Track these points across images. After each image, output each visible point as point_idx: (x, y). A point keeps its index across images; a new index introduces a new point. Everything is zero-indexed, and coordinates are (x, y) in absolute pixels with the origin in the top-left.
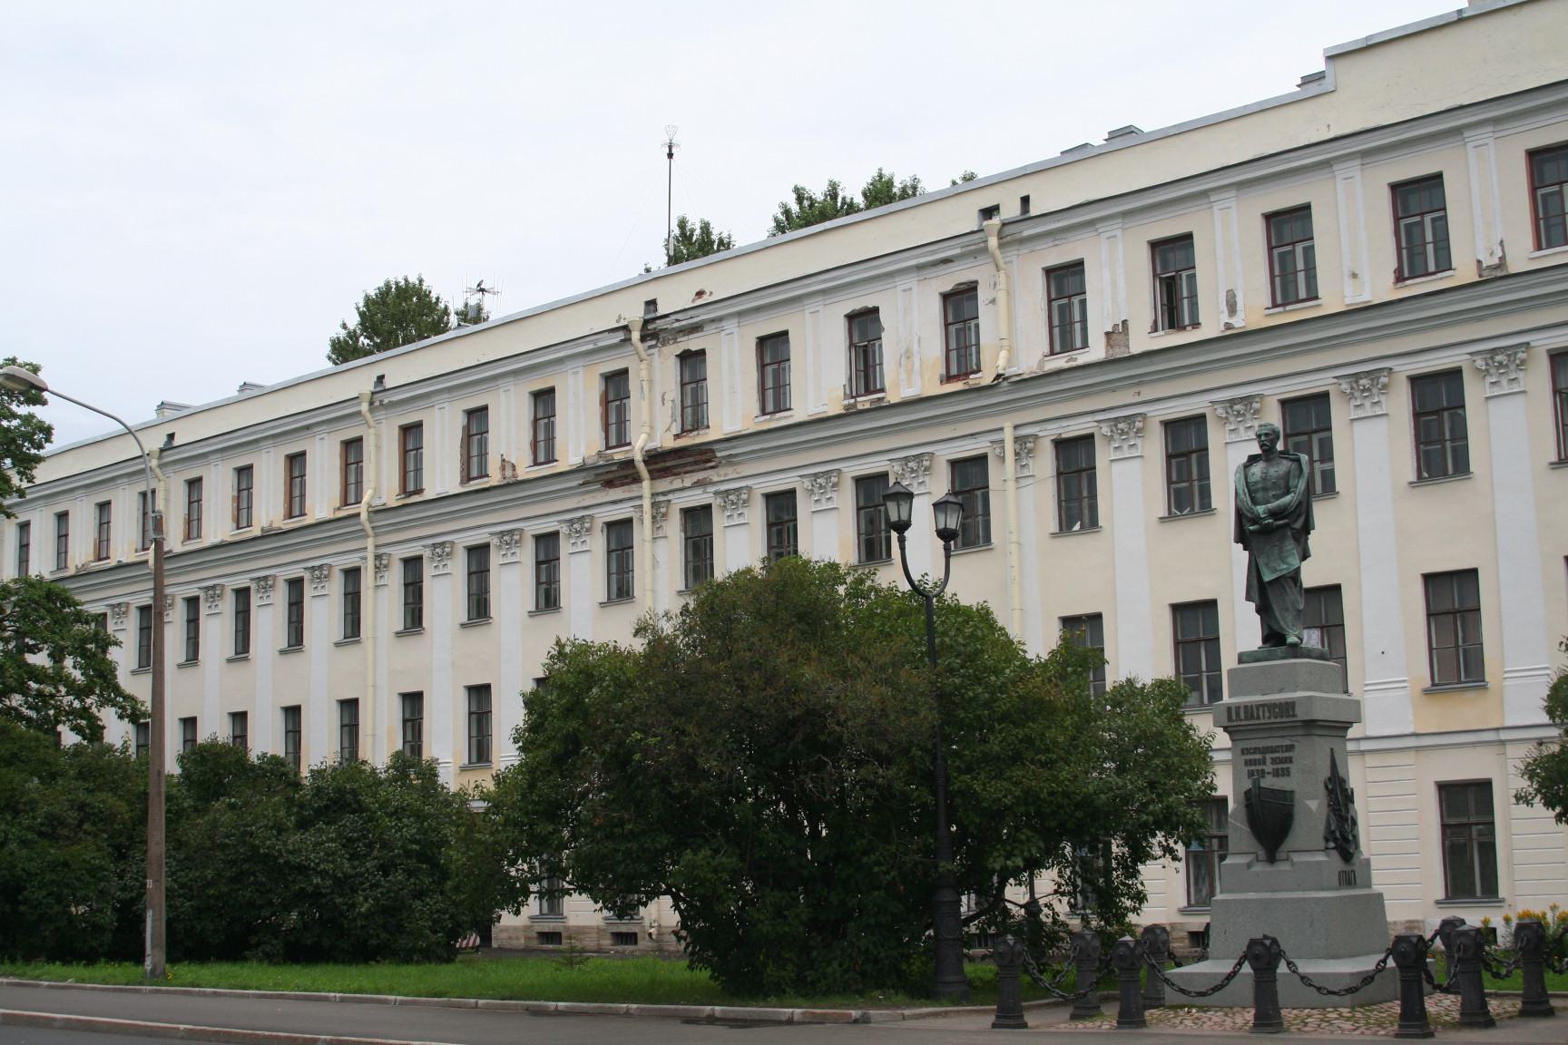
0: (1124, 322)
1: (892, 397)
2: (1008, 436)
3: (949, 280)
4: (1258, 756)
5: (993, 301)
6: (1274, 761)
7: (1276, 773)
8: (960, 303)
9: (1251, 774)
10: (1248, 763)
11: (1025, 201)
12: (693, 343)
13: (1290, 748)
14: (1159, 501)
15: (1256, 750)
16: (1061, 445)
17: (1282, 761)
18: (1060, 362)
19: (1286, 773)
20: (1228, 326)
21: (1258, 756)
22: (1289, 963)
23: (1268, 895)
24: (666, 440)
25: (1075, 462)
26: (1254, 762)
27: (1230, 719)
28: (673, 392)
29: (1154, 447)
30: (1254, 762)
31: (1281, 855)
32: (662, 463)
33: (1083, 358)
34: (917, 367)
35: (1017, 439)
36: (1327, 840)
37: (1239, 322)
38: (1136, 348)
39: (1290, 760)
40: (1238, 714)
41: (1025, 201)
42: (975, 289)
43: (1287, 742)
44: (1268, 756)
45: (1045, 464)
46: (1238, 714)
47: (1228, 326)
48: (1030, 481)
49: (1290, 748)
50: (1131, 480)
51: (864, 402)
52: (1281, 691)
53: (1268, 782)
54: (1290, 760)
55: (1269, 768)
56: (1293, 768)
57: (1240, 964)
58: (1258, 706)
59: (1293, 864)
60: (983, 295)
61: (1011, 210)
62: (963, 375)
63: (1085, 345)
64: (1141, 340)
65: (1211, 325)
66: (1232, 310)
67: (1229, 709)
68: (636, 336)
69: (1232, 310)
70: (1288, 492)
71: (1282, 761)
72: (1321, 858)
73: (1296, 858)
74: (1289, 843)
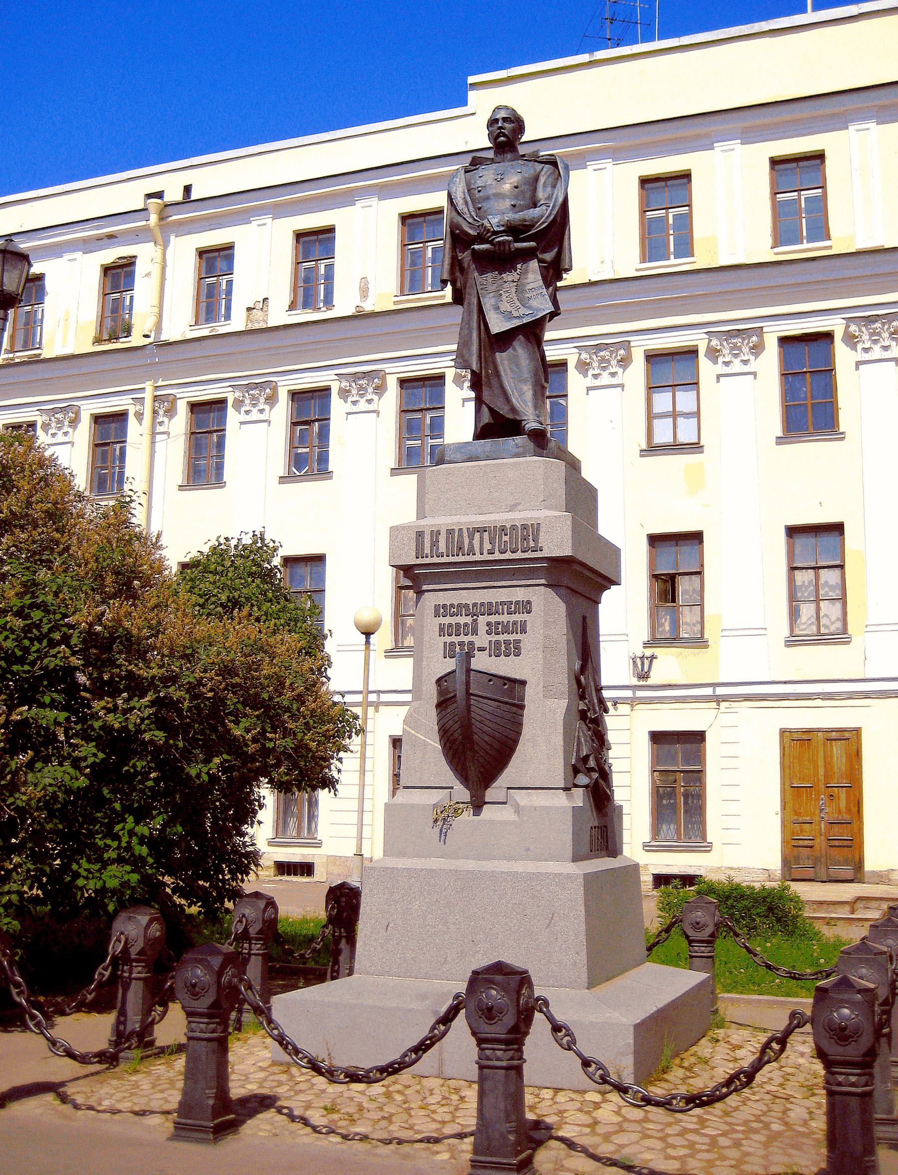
0: (265, 299)
1: (46, 353)
2: (148, 395)
3: (110, 255)
4: (463, 620)
5: (148, 275)
7: (496, 650)
8: (118, 275)
9: (449, 651)
11: (187, 189)
13: (526, 607)
14: (279, 463)
15: (462, 609)
16: (194, 407)
17: (506, 630)
19: (514, 649)
21: (463, 620)
22: (556, 1028)
23: (471, 865)
25: (208, 415)
26: (457, 630)
29: (281, 412)
35: (156, 398)
36: (576, 771)
37: (368, 307)
38: (271, 324)
40: (434, 543)
41: (187, 189)
42: (133, 264)
43: (520, 595)
44: (482, 620)
45: (179, 423)
46: (434, 543)
48: (165, 436)
50: (256, 441)
52: (512, 508)
53: (481, 662)
55: (482, 639)
56: (527, 641)
57: (447, 1019)
58: (473, 531)
59: (518, 810)
60: (140, 269)
61: (174, 194)
62: (114, 337)
63: (228, 317)
64: (279, 315)
65: (343, 306)
66: (364, 292)
67: (420, 535)
69: (364, 292)
70: (535, 205)
71: (505, 629)
72: (561, 800)
73: (520, 797)
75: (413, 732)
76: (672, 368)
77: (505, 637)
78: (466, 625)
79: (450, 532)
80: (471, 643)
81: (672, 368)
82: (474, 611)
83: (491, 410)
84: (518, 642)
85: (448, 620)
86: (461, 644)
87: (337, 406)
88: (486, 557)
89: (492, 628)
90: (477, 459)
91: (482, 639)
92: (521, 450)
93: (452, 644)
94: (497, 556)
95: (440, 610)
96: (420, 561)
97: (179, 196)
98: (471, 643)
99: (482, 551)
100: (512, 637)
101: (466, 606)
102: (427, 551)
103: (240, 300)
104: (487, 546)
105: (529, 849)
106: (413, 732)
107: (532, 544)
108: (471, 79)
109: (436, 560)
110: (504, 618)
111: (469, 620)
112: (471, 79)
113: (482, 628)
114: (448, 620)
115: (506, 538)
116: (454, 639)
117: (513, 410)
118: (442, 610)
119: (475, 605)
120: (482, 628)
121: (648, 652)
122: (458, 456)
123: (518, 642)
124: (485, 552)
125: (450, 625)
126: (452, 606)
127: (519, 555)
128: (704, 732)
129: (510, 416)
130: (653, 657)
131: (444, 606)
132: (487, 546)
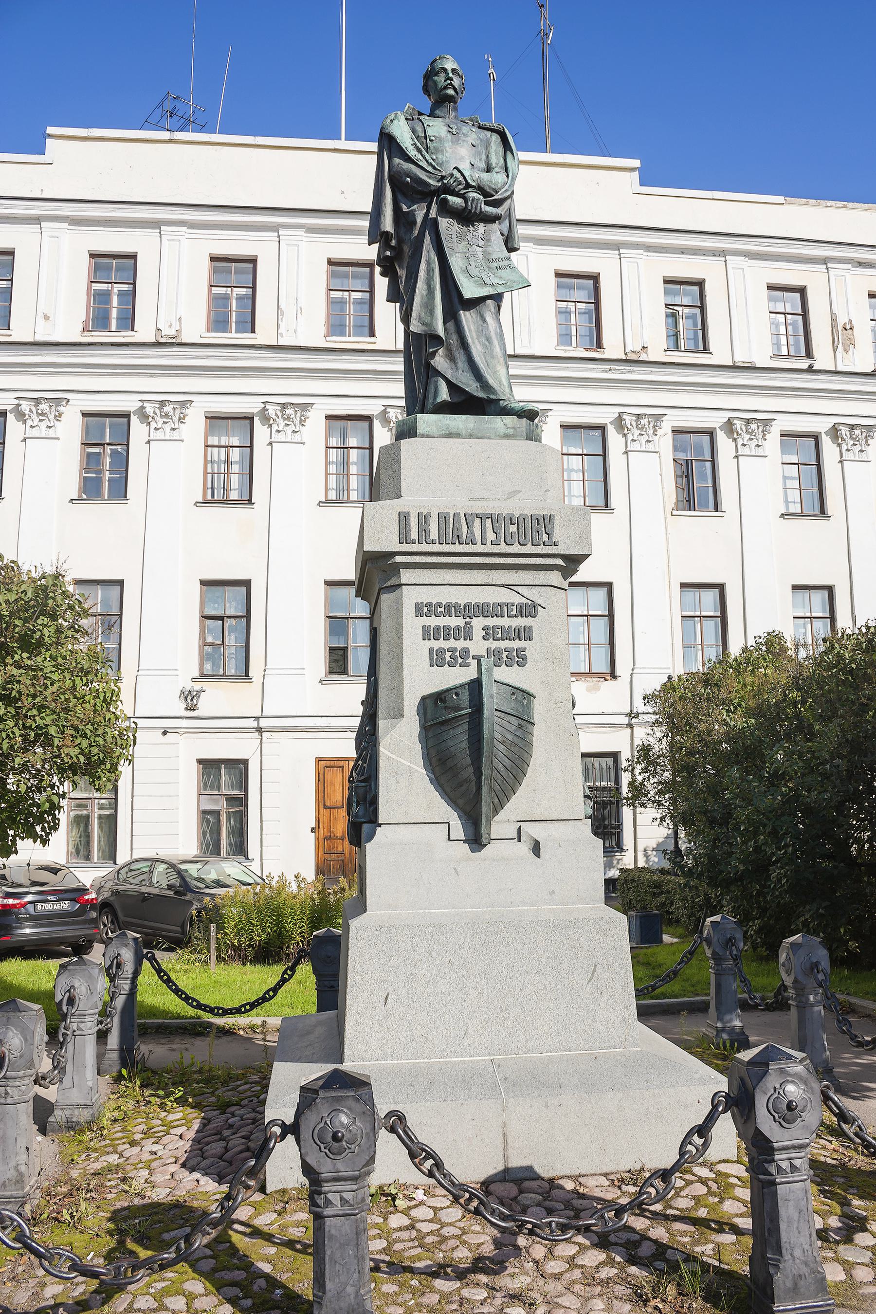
6: (489, 633)
10: (427, 634)
13: (529, 610)
15: (450, 609)
17: (507, 634)
19: (520, 659)
26: (446, 633)
27: (404, 537)
30: (446, 633)
31: (501, 825)
39: (525, 634)
40: (423, 529)
44: (478, 623)
46: (423, 529)
49: (529, 610)
54: (525, 634)
67: (404, 518)
71: (507, 634)
74: (517, 806)
75: (393, 756)
77: (506, 644)
78: (458, 628)
79: (443, 518)
80: (465, 652)
82: (471, 611)
83: (451, 386)
84: (524, 650)
85: (433, 622)
86: (453, 650)
88: (489, 548)
89: (489, 633)
90: (458, 435)
91: (478, 646)
92: (511, 431)
93: (441, 651)
94: (503, 548)
95: (419, 611)
96: (405, 548)
98: (465, 652)
99: (487, 541)
100: (516, 644)
101: (456, 606)
102: (414, 535)
104: (490, 536)
105: (553, 892)
106: (393, 756)
107: (545, 537)
109: (425, 548)
110: (505, 622)
111: (460, 622)
113: (478, 633)
114: (433, 622)
115: (513, 529)
116: (441, 644)
117: (485, 385)
118: (425, 609)
119: (468, 606)
120: (478, 633)
121: (197, 686)
122: (435, 430)
123: (524, 650)
124: (488, 542)
125: (438, 628)
126: (439, 605)
127: (529, 549)
128: (247, 760)
129: (481, 394)
130: (199, 692)
131: (429, 605)
132: (490, 536)
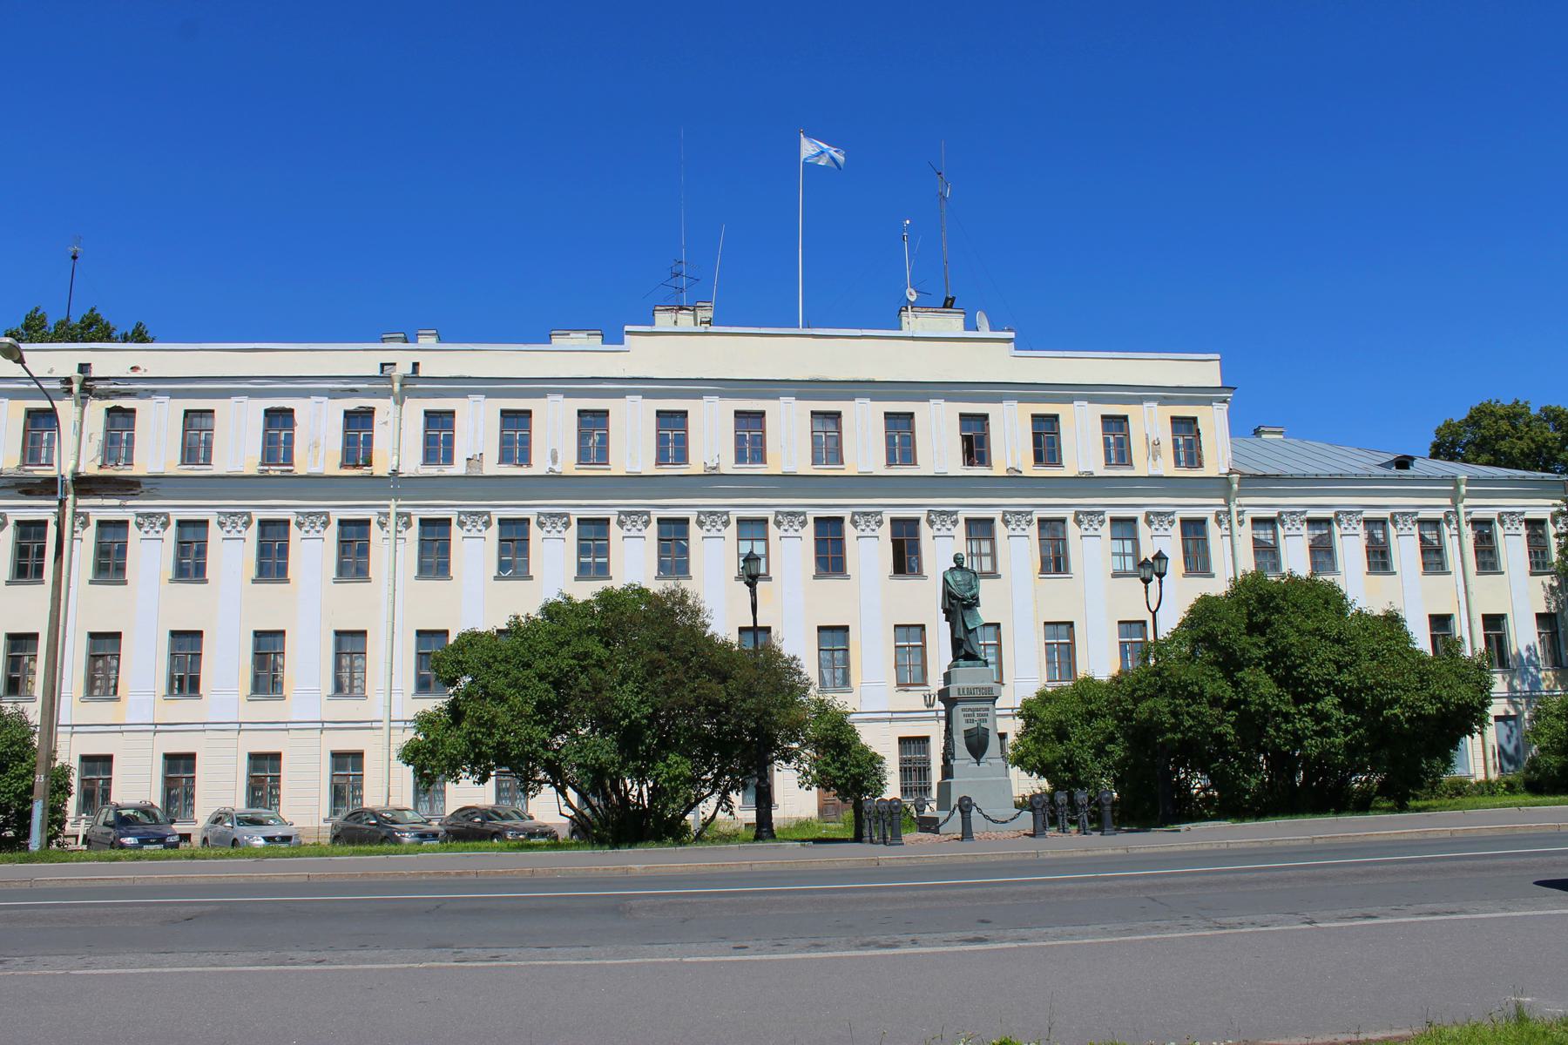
2: (393, 511)
3: (353, 404)
11: (416, 365)
12: (125, 403)
18: (432, 471)
20: (551, 470)
24: (90, 468)
28: (99, 435)
32: (85, 485)
33: (448, 471)
34: (322, 454)
35: (397, 514)
37: (558, 469)
38: (486, 472)
41: (416, 365)
47: (551, 470)
51: (275, 471)
64: (492, 467)
66: (555, 460)
68: (76, 387)
69: (554, 460)
76: (753, 527)
81: (753, 527)
87: (535, 532)
97: (409, 370)
103: (461, 451)
108: (627, 328)
112: (627, 328)
